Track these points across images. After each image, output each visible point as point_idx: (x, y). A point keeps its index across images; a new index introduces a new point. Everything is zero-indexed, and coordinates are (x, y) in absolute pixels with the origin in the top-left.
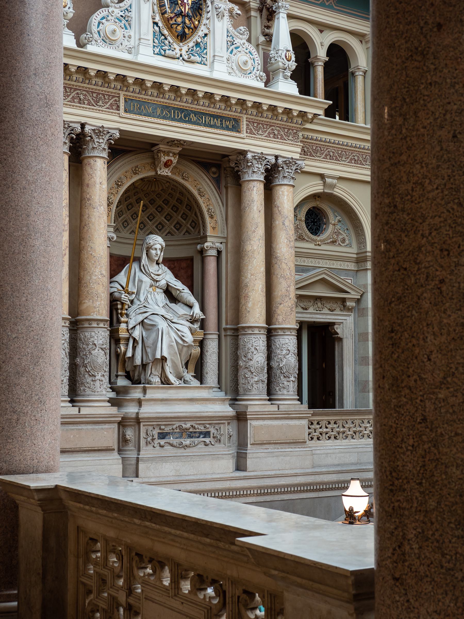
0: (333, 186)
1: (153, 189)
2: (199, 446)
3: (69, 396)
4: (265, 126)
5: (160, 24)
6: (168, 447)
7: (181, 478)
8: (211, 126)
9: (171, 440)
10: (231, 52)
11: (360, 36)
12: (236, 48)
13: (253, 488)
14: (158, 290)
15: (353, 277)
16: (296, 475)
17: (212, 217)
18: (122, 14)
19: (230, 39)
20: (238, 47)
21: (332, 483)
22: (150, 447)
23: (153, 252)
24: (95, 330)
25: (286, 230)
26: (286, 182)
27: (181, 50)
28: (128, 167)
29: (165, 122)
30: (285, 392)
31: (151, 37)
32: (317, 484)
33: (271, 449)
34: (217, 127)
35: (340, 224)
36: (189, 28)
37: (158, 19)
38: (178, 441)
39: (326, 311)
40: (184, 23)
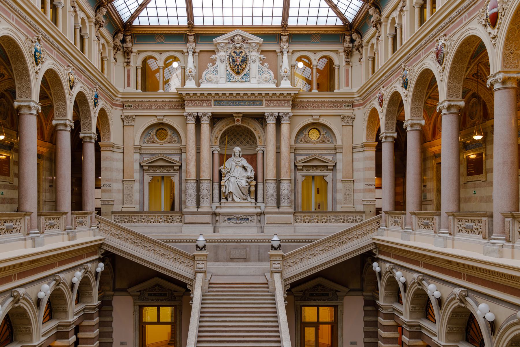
0: (318, 119)
1: (238, 129)
2: (244, 223)
3: (196, 205)
4: (274, 101)
5: (229, 70)
6: (231, 223)
7: (235, 234)
8: (250, 105)
9: (233, 221)
10: (260, 75)
11: (336, 52)
12: (262, 72)
13: (267, 240)
14: (239, 167)
15: (334, 156)
16: (286, 236)
17: (259, 138)
18: (214, 70)
19: (260, 69)
20: (264, 72)
21: (304, 240)
22: (224, 223)
23: (236, 153)
24: (204, 183)
25: (284, 141)
26: (284, 122)
27: (238, 78)
28: (224, 124)
29: (230, 107)
30: (283, 204)
31: (225, 76)
32: (296, 239)
33: (275, 225)
34: (252, 105)
35: (327, 134)
36: (240, 69)
37: (228, 68)
38: (235, 221)
39: (319, 171)
40: (238, 68)
